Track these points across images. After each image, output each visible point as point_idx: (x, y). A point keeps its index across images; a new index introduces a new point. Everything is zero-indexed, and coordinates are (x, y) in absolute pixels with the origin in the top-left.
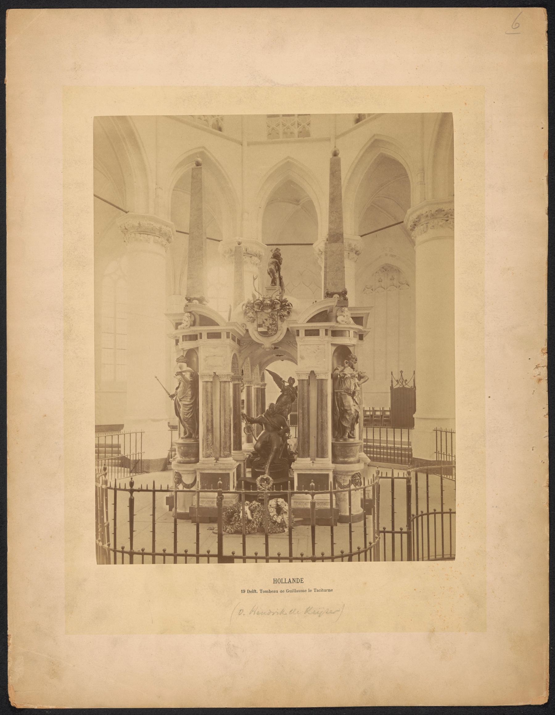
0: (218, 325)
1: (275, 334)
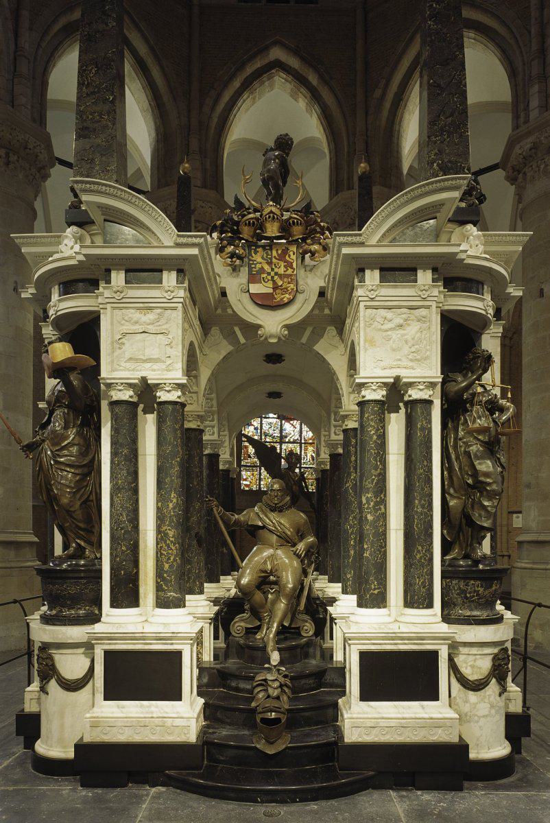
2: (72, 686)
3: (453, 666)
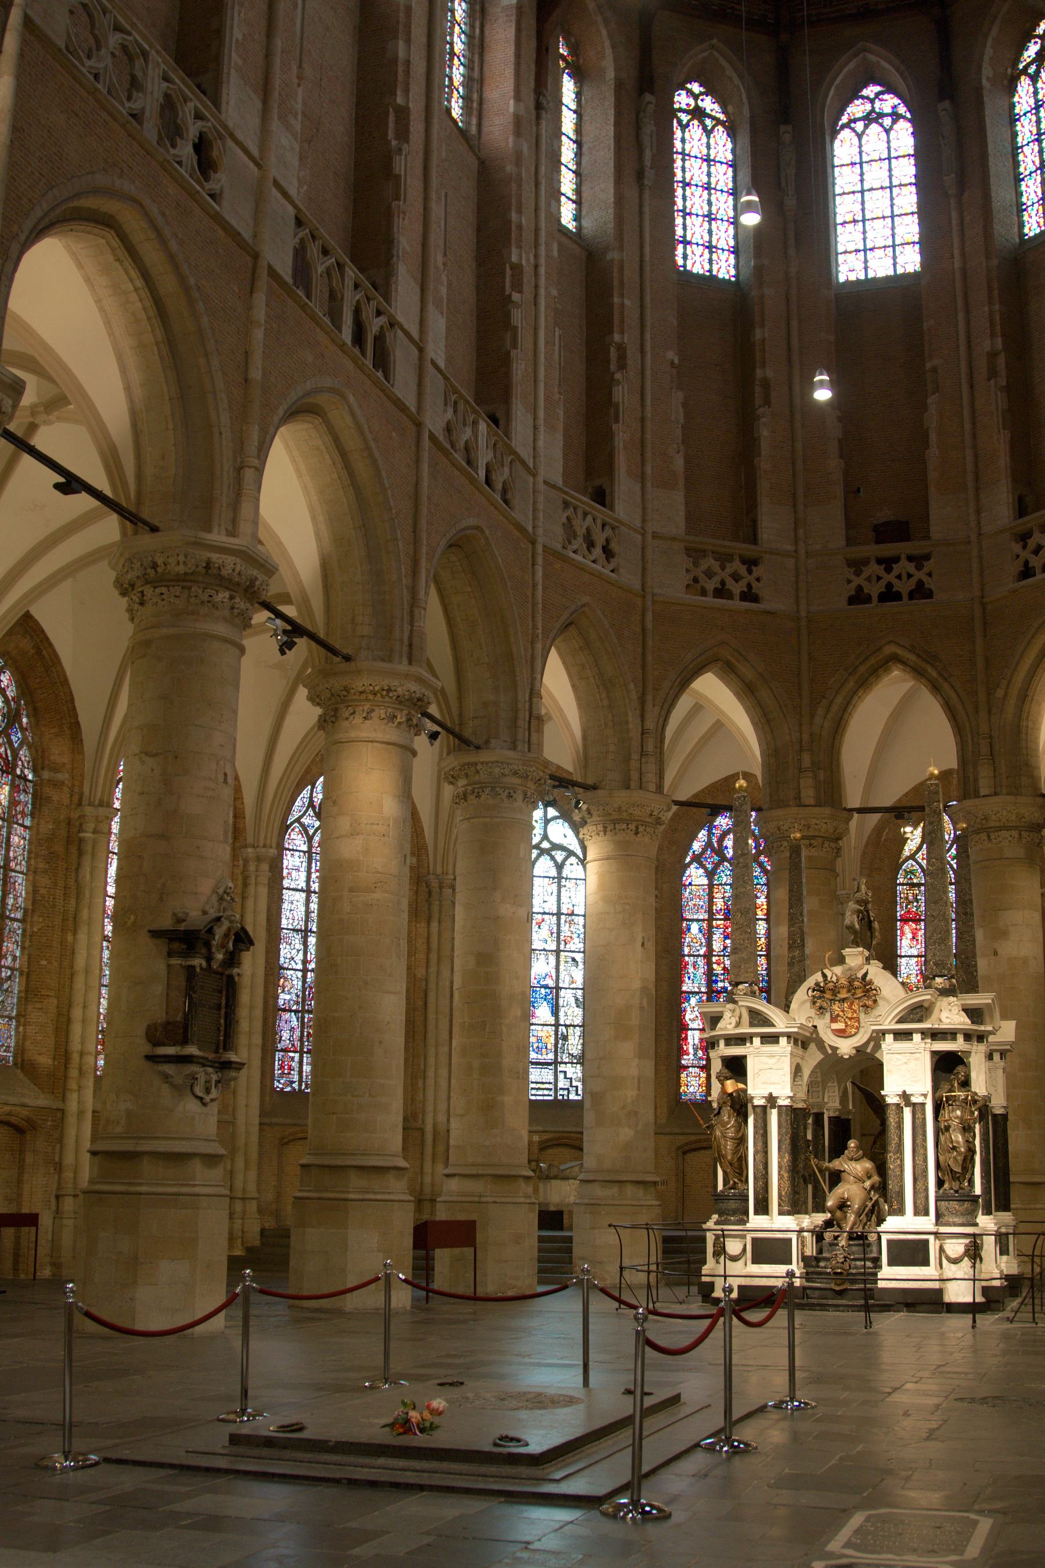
0: (773, 1025)
1: (856, 1034)
2: (734, 1259)
3: (942, 1250)
